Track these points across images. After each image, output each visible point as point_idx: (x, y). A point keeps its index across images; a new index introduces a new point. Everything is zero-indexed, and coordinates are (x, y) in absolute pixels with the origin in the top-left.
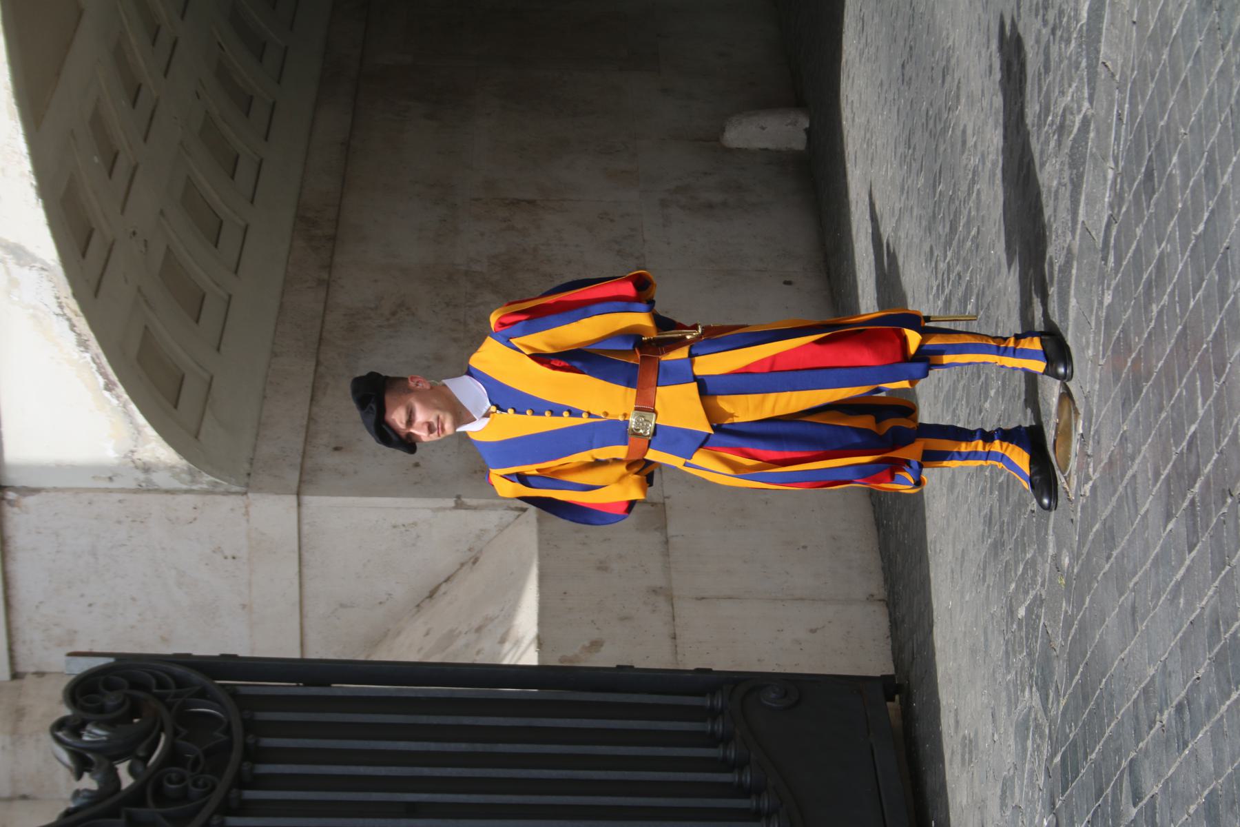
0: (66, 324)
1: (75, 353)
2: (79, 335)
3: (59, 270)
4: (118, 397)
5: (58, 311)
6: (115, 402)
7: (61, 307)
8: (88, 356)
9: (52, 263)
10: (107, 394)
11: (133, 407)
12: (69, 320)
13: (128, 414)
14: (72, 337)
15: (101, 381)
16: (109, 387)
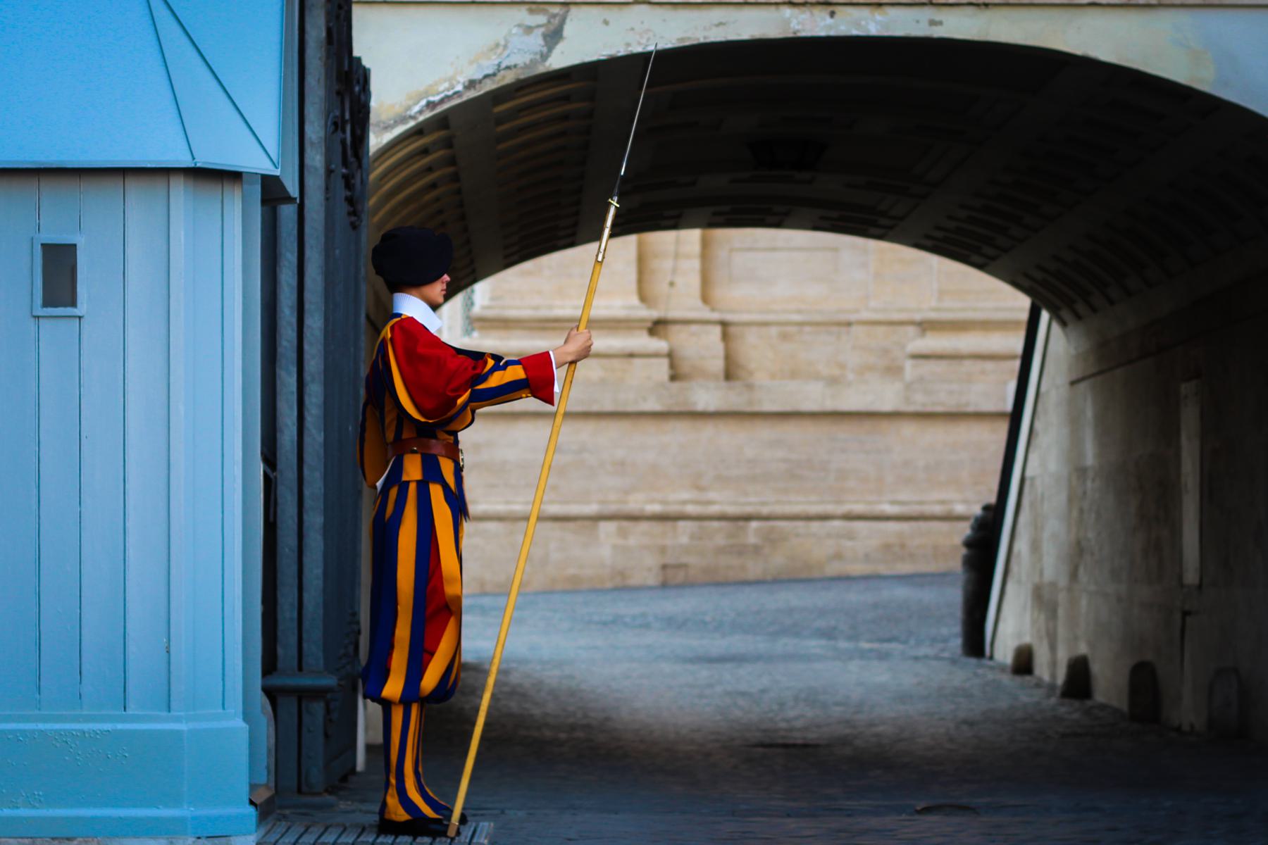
0: (490, 71)
1: (463, 79)
2: (480, 81)
3: (541, 69)
4: (421, 112)
5: (503, 65)
6: (416, 109)
7: (508, 68)
8: (459, 88)
9: (547, 64)
10: (424, 102)
11: (412, 124)
12: (494, 75)
13: (403, 120)
14: (479, 76)
15: (436, 98)
16: (431, 105)
